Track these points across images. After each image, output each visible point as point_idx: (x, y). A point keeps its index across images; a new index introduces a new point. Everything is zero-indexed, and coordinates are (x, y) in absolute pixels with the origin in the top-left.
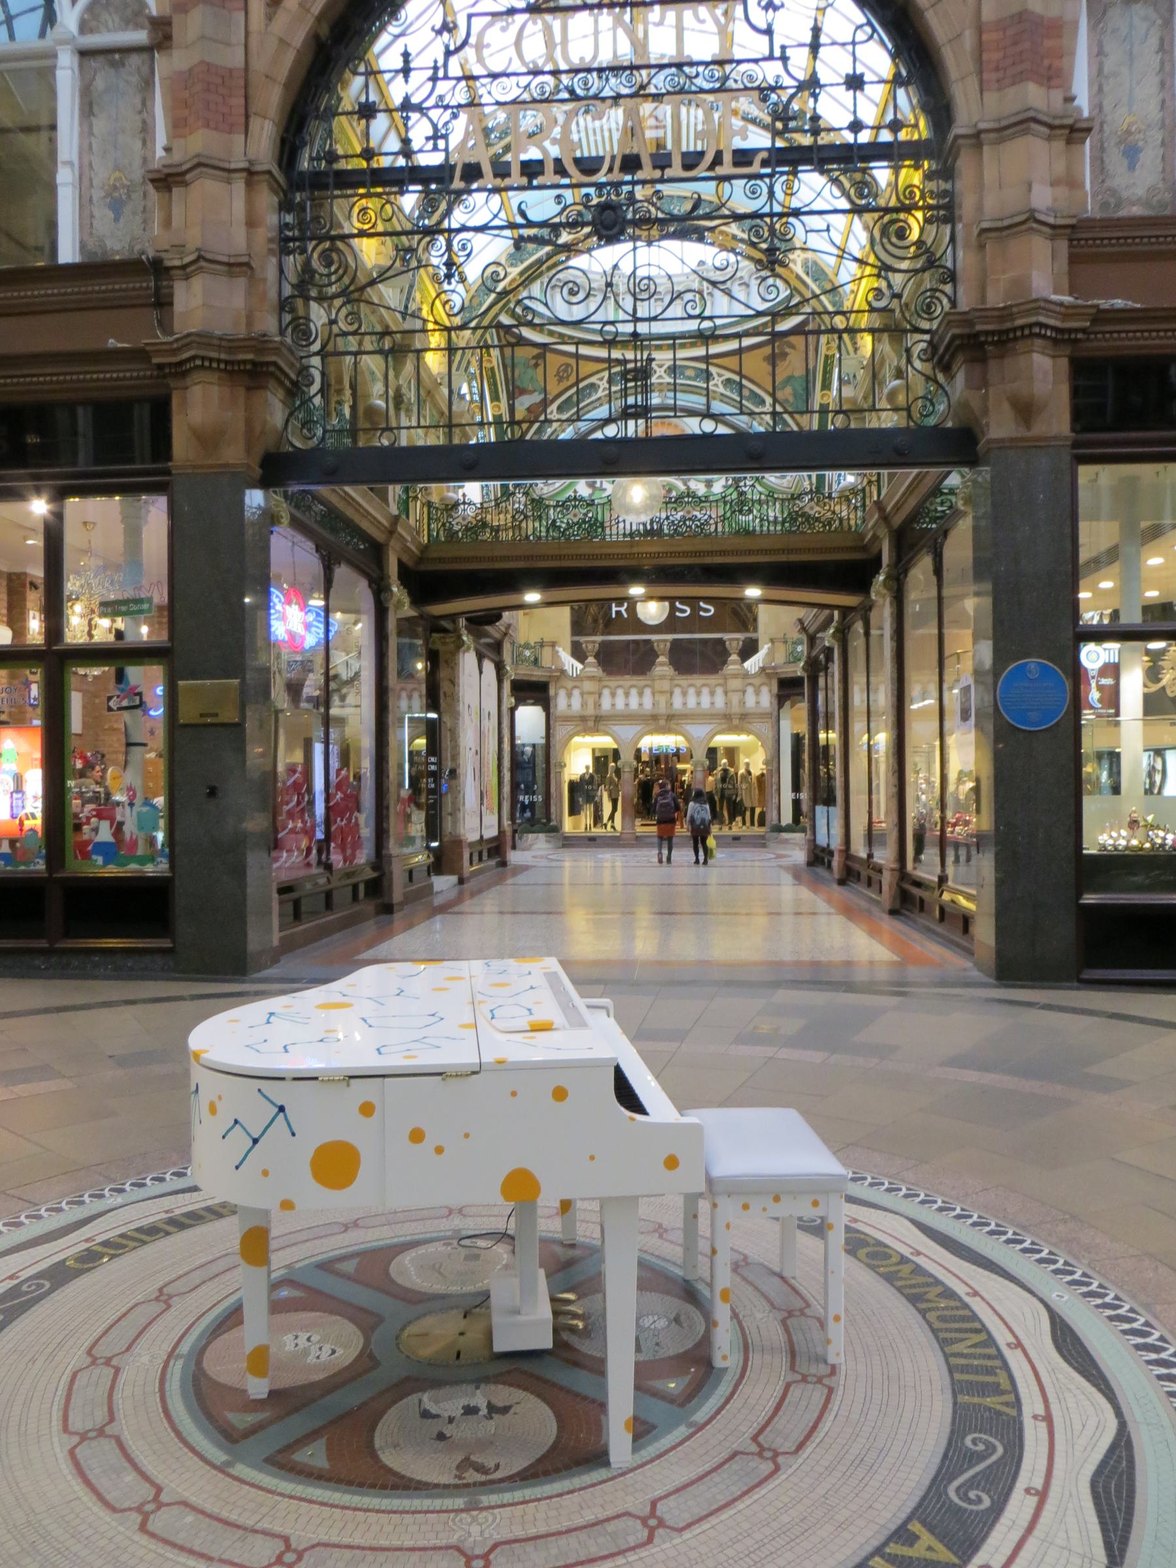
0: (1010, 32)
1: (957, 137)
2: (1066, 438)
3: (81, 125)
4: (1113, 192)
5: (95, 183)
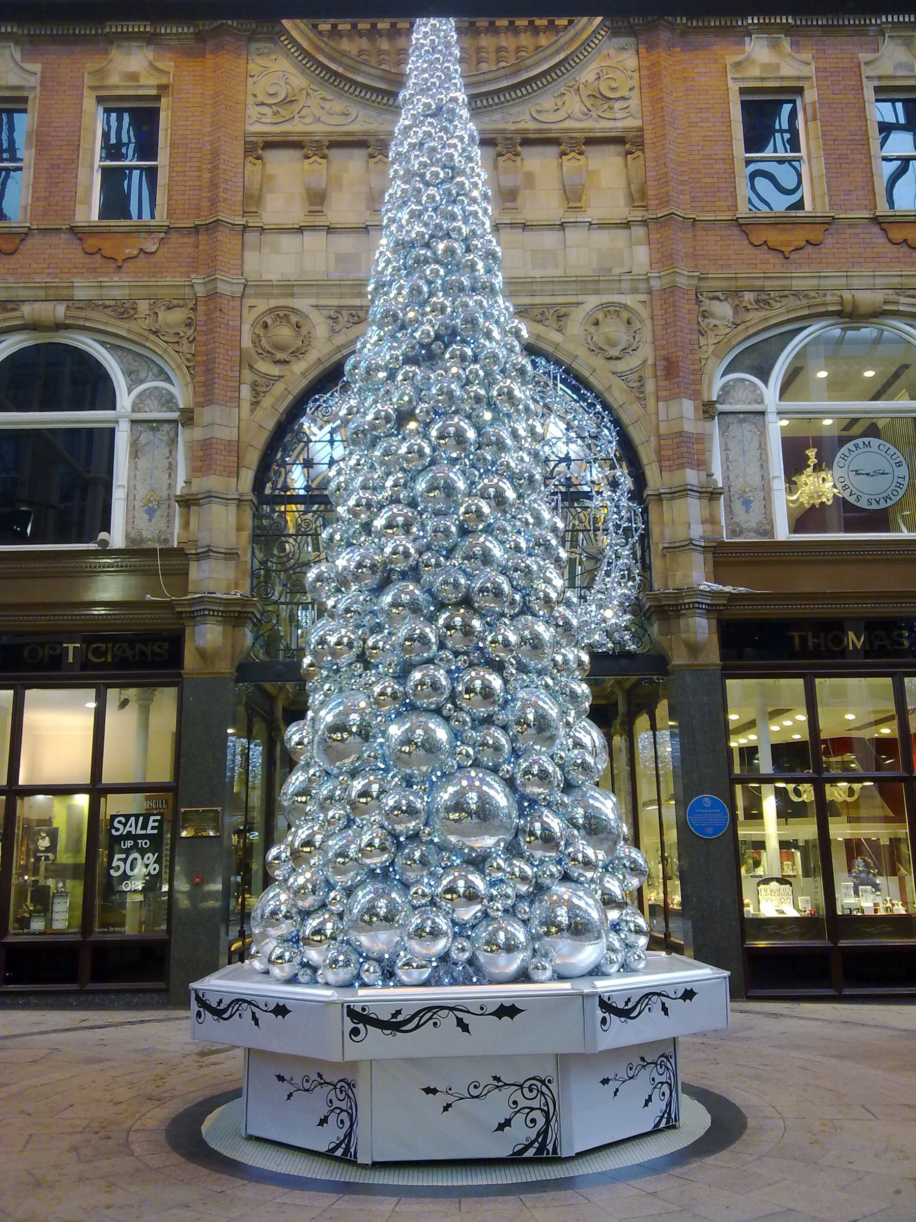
0: (675, 441)
1: (648, 495)
2: (718, 665)
4: (738, 525)
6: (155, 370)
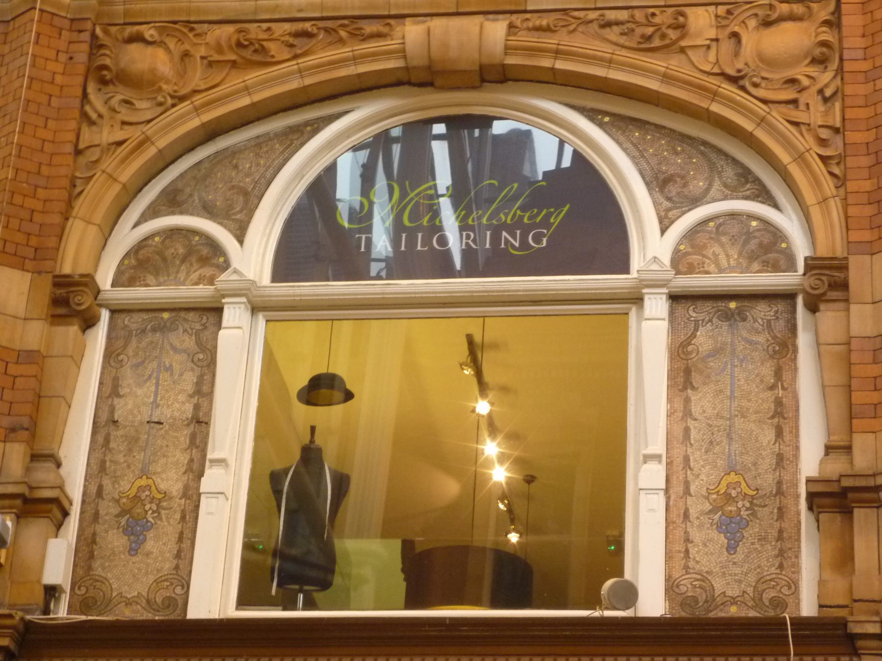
3: (670, 400)
5: (692, 489)
6: (729, 173)
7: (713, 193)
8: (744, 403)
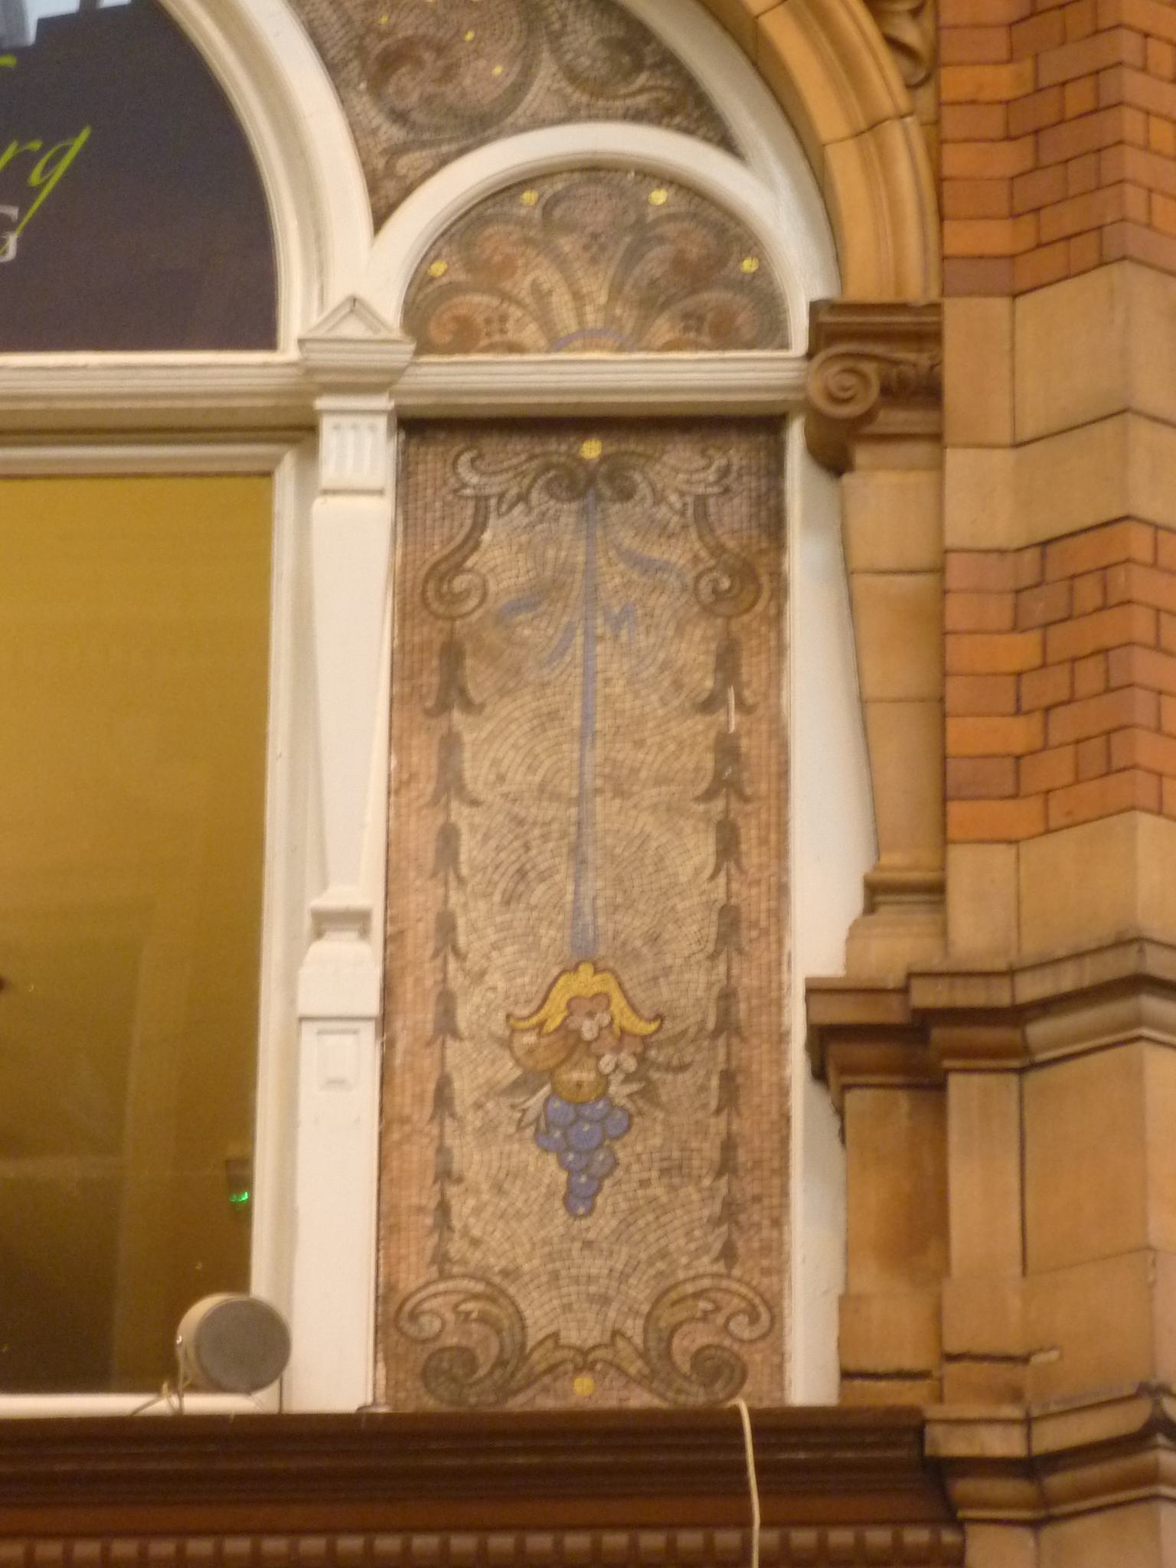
3: (396, 742)
5: (464, 1016)
7: (535, 97)
8: (624, 753)
